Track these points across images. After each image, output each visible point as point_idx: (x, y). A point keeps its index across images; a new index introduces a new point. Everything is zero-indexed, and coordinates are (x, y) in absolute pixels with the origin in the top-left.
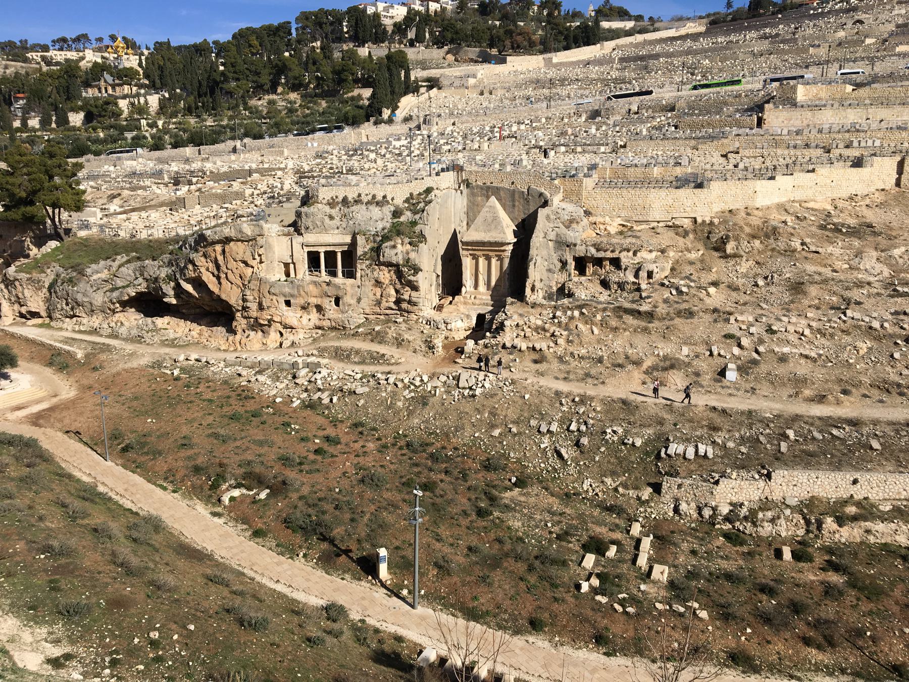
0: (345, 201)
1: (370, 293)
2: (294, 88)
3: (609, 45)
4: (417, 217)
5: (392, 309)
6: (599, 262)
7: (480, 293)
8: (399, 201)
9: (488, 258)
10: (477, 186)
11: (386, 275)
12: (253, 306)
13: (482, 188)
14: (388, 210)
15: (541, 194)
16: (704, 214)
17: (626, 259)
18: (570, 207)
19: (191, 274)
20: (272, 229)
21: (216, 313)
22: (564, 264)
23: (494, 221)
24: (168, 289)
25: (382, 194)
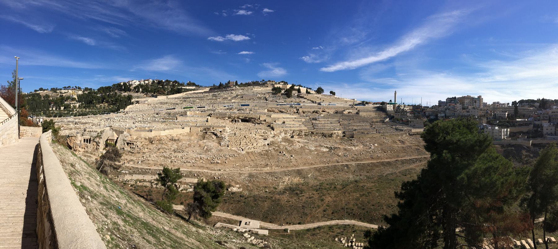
1: (92, 146)
2: (107, 102)
6: (130, 144)
11: (95, 144)
16: (150, 137)
17: (135, 143)
20: (79, 135)
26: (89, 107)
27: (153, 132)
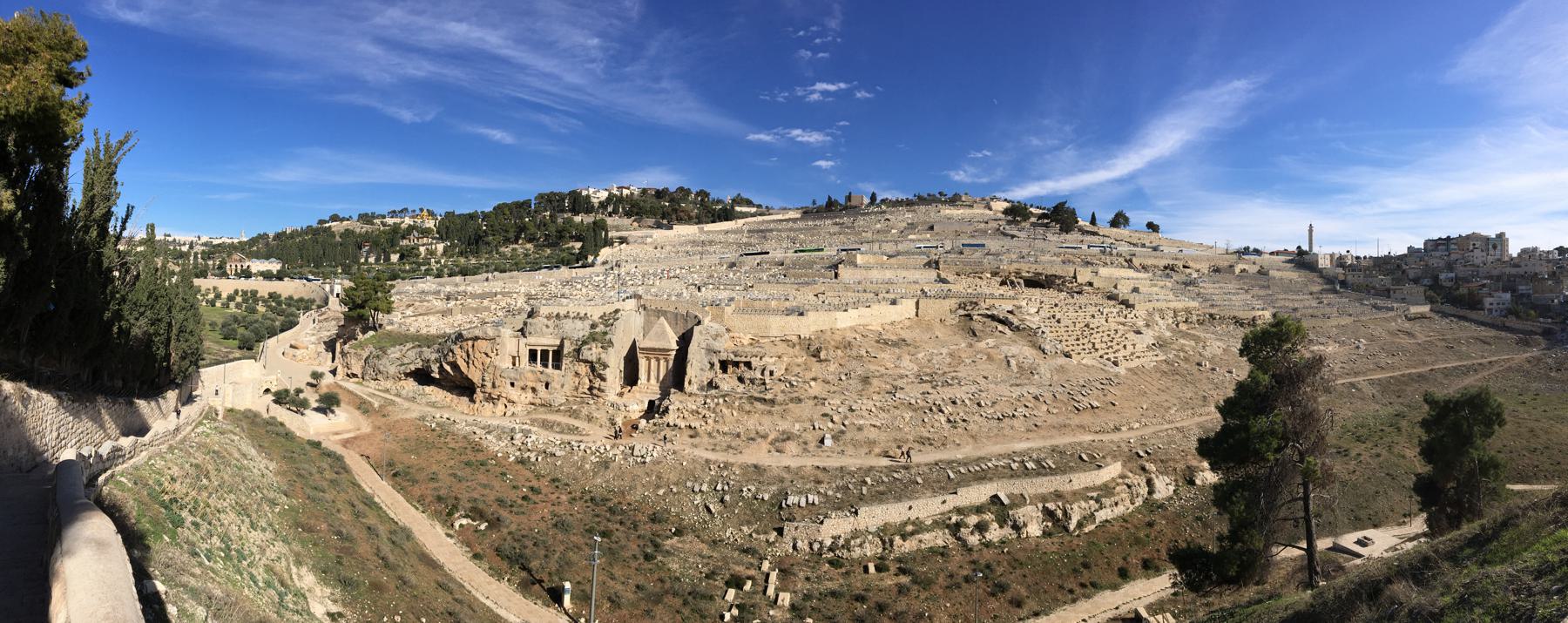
0: (558, 316)
1: (571, 381)
3: (741, 222)
6: (736, 364)
8: (596, 318)
9: (658, 360)
11: (583, 369)
12: (489, 385)
14: (588, 323)
16: (805, 333)
17: (755, 362)
18: (716, 326)
19: (450, 359)
21: (464, 387)
22: (712, 365)
23: (663, 334)
24: (435, 368)
26: (476, 253)
27: (812, 316)
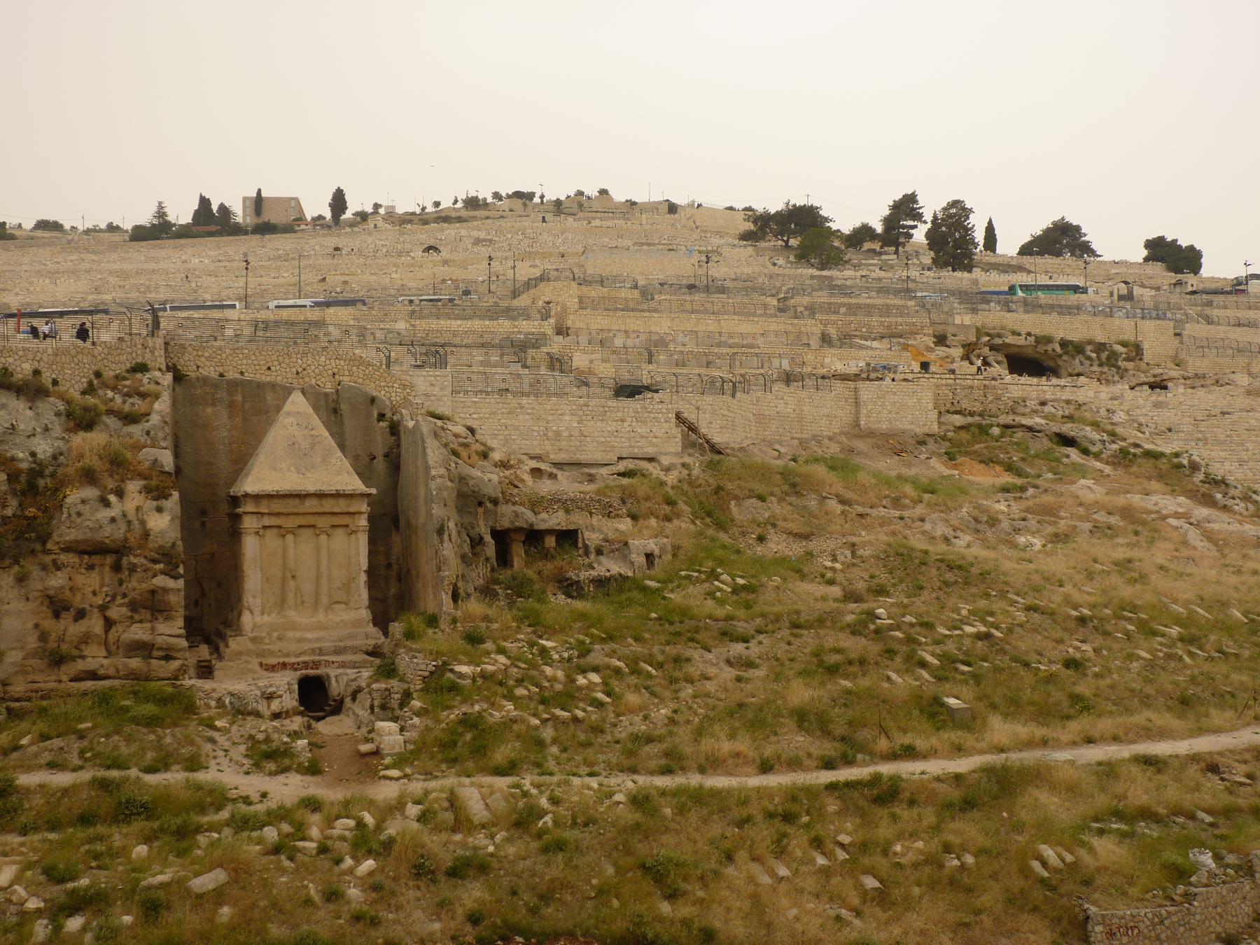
4: (136, 430)
5: (93, 676)
7: (294, 626)
10: (205, 381)
13: (216, 386)
15: (373, 400)
22: (477, 542)
25: (27, 367)
